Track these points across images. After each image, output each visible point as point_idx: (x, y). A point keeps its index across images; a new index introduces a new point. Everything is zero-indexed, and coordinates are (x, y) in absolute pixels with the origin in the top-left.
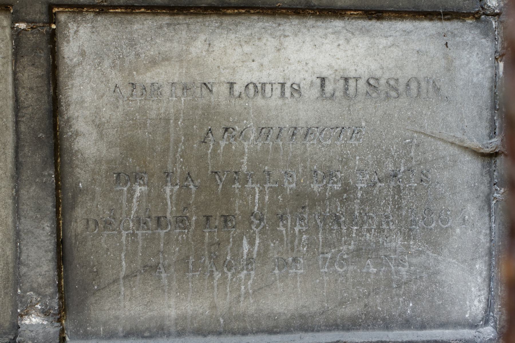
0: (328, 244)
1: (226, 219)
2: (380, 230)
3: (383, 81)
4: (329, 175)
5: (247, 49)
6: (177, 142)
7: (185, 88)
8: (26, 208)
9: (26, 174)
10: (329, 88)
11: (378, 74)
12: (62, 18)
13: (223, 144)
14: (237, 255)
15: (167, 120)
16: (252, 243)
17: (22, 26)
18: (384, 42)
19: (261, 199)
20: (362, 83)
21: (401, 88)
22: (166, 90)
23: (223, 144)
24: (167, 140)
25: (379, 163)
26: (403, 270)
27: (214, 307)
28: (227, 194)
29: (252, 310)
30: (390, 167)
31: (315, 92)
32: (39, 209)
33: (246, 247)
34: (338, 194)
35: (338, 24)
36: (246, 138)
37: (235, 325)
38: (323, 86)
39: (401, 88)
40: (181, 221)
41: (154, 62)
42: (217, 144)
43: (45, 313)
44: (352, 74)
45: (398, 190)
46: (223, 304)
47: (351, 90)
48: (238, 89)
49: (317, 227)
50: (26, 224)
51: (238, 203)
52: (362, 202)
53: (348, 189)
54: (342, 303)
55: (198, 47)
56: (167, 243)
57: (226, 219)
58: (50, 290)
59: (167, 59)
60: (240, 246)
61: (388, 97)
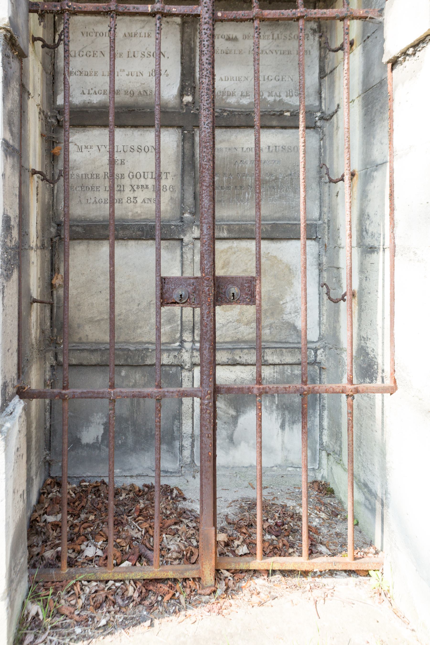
0: (271, 195)
1: (241, 187)
2: (286, 191)
3: (287, 147)
4: (271, 174)
5: (247, 138)
6: (227, 165)
7: (229, 149)
8: (186, 182)
9: (186, 173)
10: (271, 149)
11: (285, 145)
12: (196, 130)
13: (240, 165)
14: (244, 198)
15: (224, 159)
16: (249, 194)
17: (186, 132)
18: (287, 136)
19: (251, 181)
20: (280, 148)
21: (292, 149)
22: (224, 150)
23: (240, 165)
24: (224, 164)
25: (286, 171)
26: (294, 203)
27: (238, 213)
28: (241, 180)
29: (249, 214)
30: (289, 172)
31: (267, 150)
32: (189, 183)
33: (247, 195)
34: (274, 180)
35: (273, 131)
36: (247, 164)
37: (244, 219)
38: (269, 148)
39: (292, 149)
40: (228, 188)
41: (221, 142)
42: (238, 166)
43: (190, 213)
44: (277, 145)
45: (292, 179)
46: (240, 212)
47: (277, 150)
48: (244, 149)
49: (268, 190)
50: (185, 187)
51: (245, 182)
52: (281, 183)
53: (277, 179)
54: (275, 213)
55: (233, 138)
56: (224, 194)
57: (241, 187)
58: (192, 206)
59: (224, 141)
60: (245, 195)
61: (288, 151)
